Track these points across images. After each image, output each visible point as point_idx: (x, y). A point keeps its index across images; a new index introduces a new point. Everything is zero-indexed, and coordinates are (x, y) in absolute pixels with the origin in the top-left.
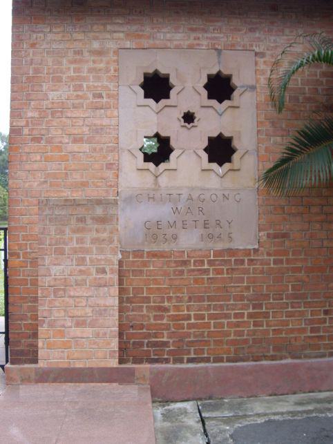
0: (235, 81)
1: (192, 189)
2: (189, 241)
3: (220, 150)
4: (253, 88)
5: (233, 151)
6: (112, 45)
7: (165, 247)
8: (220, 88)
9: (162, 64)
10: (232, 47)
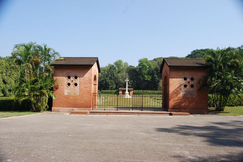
0: (194, 78)
1: (189, 90)
2: (189, 96)
3: (192, 86)
4: (196, 79)
5: (194, 86)
8: (192, 79)
9: (186, 76)
10: (194, 74)
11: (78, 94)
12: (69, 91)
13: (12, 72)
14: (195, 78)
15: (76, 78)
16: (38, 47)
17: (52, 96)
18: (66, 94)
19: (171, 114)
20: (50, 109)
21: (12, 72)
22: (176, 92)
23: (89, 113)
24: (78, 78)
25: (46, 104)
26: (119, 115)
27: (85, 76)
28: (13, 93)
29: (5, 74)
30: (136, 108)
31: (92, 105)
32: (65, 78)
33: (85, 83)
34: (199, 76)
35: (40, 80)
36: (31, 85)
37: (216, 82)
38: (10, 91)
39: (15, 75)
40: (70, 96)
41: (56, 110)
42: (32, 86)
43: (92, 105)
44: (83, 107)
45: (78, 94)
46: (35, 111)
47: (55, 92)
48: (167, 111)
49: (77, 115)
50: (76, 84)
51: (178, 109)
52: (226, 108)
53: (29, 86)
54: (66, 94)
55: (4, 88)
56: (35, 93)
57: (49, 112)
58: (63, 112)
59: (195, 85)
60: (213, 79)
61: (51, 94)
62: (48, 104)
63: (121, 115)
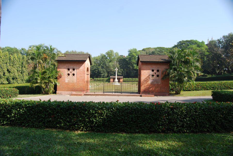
0: (159, 70)
2: (155, 83)
3: (158, 76)
6: (149, 67)
7: (153, 83)
8: (158, 71)
11: (75, 81)
12: (69, 79)
13: (15, 62)
14: (160, 70)
15: (74, 70)
16: (46, 47)
17: (56, 83)
18: (67, 81)
19: (141, 96)
20: (55, 92)
21: (15, 62)
22: (146, 80)
23: (83, 95)
24: (75, 70)
25: (52, 89)
26: (105, 96)
27: (80, 68)
28: (16, 81)
29: (9, 64)
30: (117, 92)
31: (85, 90)
32: (66, 70)
33: (80, 74)
34: (162, 68)
35: (48, 72)
36: (41, 75)
37: (174, 73)
38: (13, 79)
39: (17, 65)
40: (70, 83)
41: (59, 93)
42: (42, 76)
43: (85, 90)
44: (79, 91)
45: (75, 81)
46: (44, 94)
47: (59, 80)
48: (140, 94)
49: (75, 96)
50: (74, 75)
51: (147, 92)
52: (182, 92)
53: (40, 76)
54: (67, 81)
55: (8, 77)
56: (45, 81)
57: (55, 95)
58: (64, 94)
59: (160, 75)
60: (171, 71)
61: (56, 81)
62: (54, 89)
63: (106, 97)
